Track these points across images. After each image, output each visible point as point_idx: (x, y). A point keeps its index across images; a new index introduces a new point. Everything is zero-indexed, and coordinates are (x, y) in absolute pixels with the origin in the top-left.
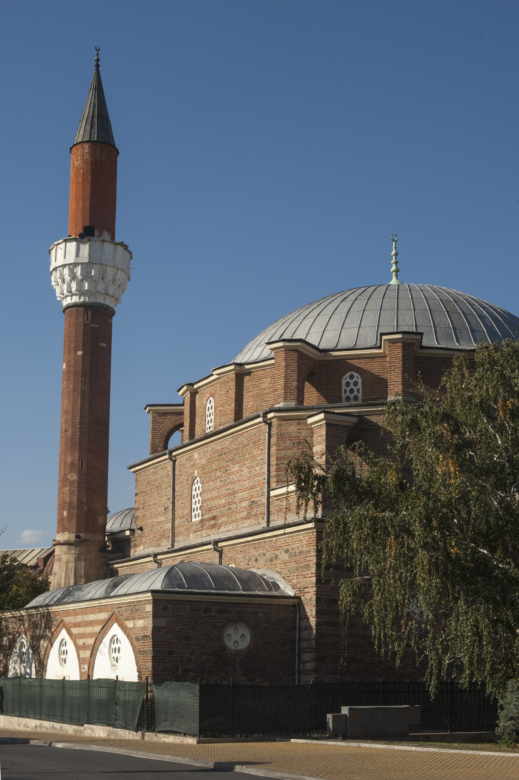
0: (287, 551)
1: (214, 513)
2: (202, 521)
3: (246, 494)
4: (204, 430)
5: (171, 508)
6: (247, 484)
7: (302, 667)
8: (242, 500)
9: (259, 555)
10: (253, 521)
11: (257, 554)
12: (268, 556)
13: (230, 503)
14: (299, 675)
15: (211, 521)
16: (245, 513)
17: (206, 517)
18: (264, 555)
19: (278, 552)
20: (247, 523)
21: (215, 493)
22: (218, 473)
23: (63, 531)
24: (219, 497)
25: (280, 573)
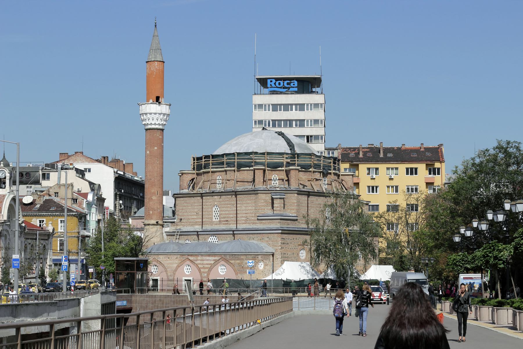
1: (227, 219)
6: (244, 212)
10: (248, 225)
20: (245, 225)
21: (227, 212)
22: (229, 206)
24: (230, 214)
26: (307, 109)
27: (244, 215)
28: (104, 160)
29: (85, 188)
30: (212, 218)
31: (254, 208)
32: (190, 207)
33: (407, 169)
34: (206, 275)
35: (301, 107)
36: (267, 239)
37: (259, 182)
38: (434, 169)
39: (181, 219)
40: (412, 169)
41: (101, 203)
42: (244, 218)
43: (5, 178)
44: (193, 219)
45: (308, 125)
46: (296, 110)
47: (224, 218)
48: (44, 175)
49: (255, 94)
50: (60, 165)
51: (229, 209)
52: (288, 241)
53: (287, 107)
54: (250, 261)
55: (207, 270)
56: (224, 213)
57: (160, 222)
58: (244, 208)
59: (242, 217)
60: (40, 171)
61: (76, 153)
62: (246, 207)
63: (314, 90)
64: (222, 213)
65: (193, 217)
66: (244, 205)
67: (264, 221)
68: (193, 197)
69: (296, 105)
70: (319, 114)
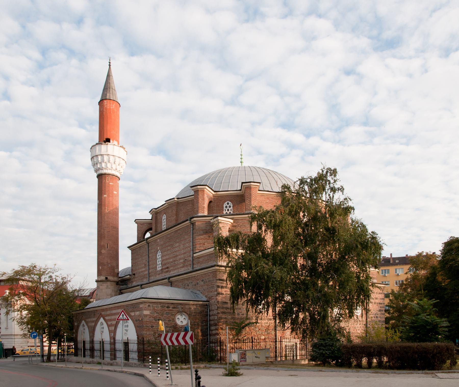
0: (202, 281)
1: (167, 266)
2: (162, 269)
3: (182, 256)
4: (162, 229)
5: (147, 264)
7: (211, 333)
8: (180, 259)
9: (189, 283)
11: (188, 283)
12: (194, 283)
13: (175, 261)
14: (210, 336)
15: (166, 269)
16: (182, 265)
17: (164, 267)
18: (192, 283)
19: (198, 281)
20: (183, 269)
21: (167, 257)
22: (169, 248)
25: (200, 291)
30: (156, 267)
34: (113, 334)
36: (202, 283)
39: (134, 274)
44: (142, 272)
47: (165, 264)
51: (169, 252)
55: (113, 328)
57: (110, 278)
58: (182, 246)
62: (184, 244)
64: (163, 258)
66: (183, 243)
67: (201, 260)
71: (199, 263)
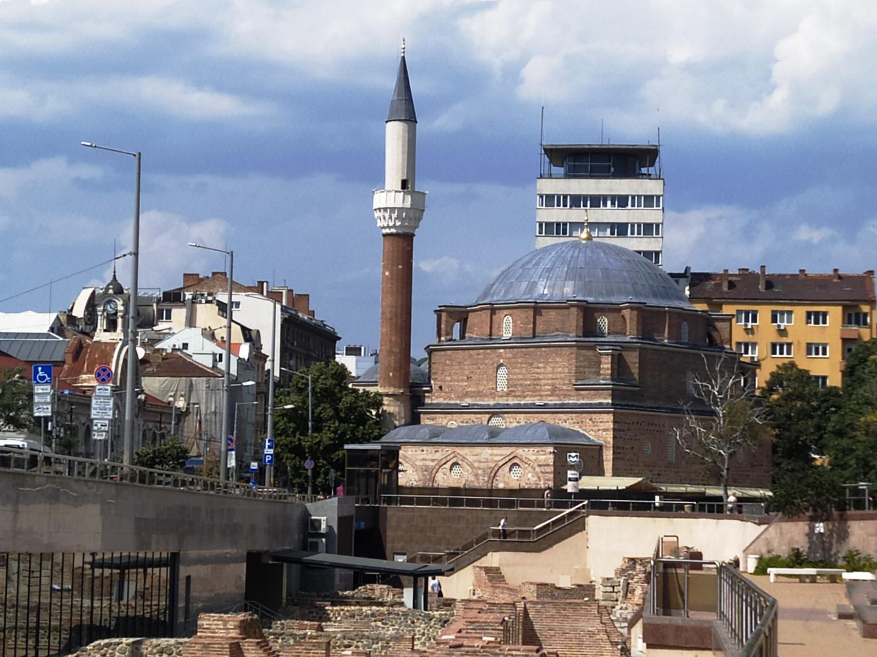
20: (551, 398)
21: (520, 377)
23: (389, 386)
24: (526, 380)
26: (633, 205)
27: (549, 382)
28: (259, 289)
29: (237, 335)
31: (566, 370)
32: (456, 367)
33: (809, 314)
35: (622, 201)
37: (577, 326)
38: (857, 315)
40: (817, 314)
41: (261, 363)
42: (550, 387)
43: (116, 314)
45: (632, 233)
46: (613, 204)
48: (160, 312)
49: (541, 177)
50: (188, 296)
51: (524, 371)
52: (625, 427)
53: (596, 201)
54: (573, 454)
56: (515, 377)
58: (549, 369)
59: (547, 384)
60: (155, 305)
61: (214, 274)
62: (553, 368)
63: (644, 170)
64: (511, 376)
65: (460, 384)
68: (522, 338)
69: (613, 198)
70: (651, 215)
71: (580, 395)
